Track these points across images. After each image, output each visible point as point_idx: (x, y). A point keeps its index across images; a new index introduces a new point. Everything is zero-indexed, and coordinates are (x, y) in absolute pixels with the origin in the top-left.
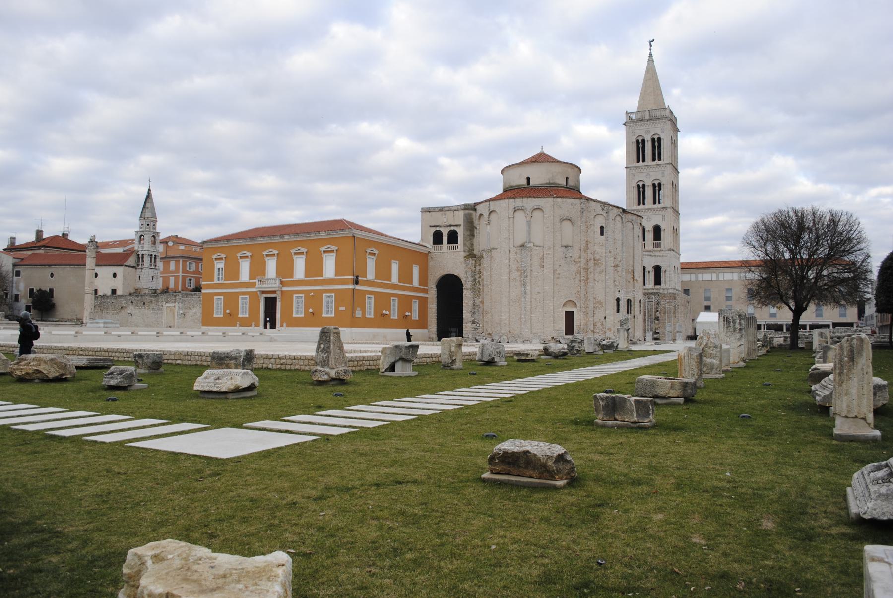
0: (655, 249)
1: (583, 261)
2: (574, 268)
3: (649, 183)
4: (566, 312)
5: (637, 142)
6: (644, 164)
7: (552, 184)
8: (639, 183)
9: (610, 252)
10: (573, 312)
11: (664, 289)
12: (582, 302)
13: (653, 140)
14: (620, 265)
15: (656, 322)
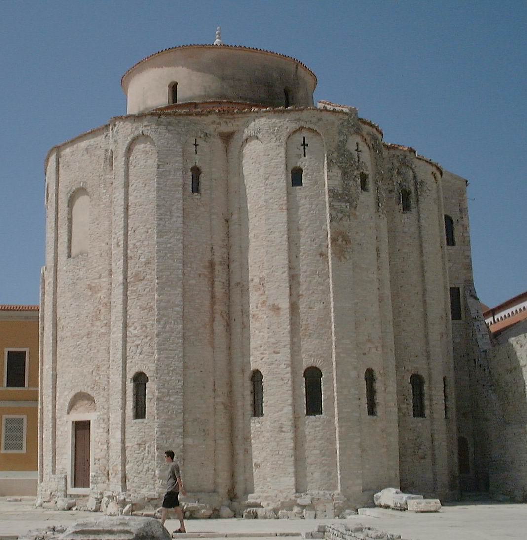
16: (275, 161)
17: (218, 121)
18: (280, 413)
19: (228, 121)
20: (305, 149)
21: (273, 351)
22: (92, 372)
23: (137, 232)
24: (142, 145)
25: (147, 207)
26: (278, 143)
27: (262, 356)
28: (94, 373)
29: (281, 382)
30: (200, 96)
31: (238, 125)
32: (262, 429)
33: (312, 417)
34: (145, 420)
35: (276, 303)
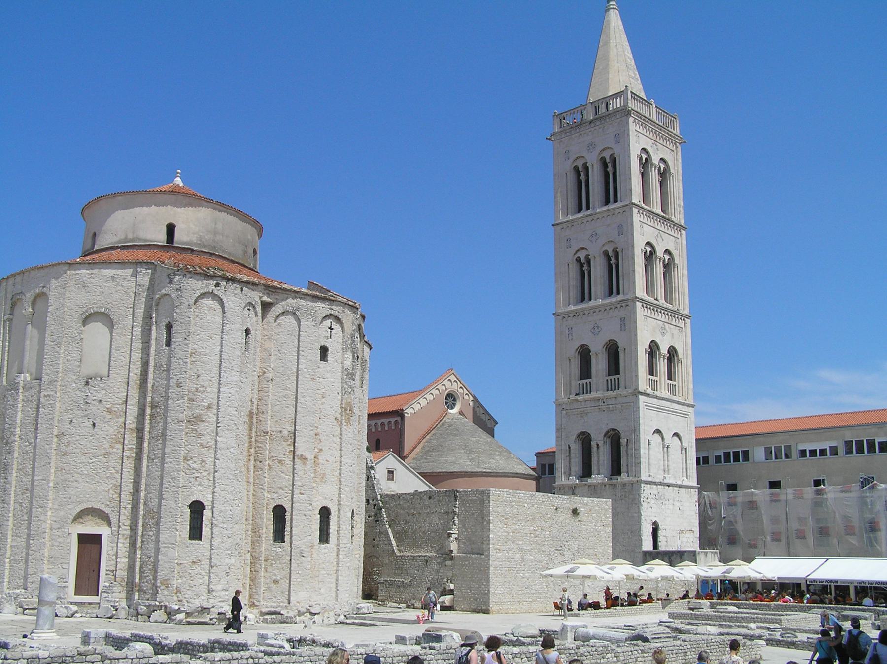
0: (610, 393)
1: (133, 410)
2: (109, 429)
3: (595, 251)
4: (79, 535)
5: (576, 169)
6: (589, 212)
7: (132, 241)
8: (578, 255)
9: (179, 385)
10: (100, 537)
11: (624, 485)
12: (123, 511)
13: (604, 164)
14: (211, 416)
15: (449, 563)
16: (311, 338)
17: (263, 291)
18: (302, 541)
19: (270, 293)
20: (331, 332)
21: (298, 492)
22: (109, 489)
23: (200, 378)
24: (211, 302)
25: (212, 358)
26: (313, 323)
27: (287, 495)
28: (111, 491)
29: (304, 517)
30: (196, 244)
31: (277, 299)
32: (284, 553)
33: (323, 546)
34: (201, 543)
35: (304, 454)
